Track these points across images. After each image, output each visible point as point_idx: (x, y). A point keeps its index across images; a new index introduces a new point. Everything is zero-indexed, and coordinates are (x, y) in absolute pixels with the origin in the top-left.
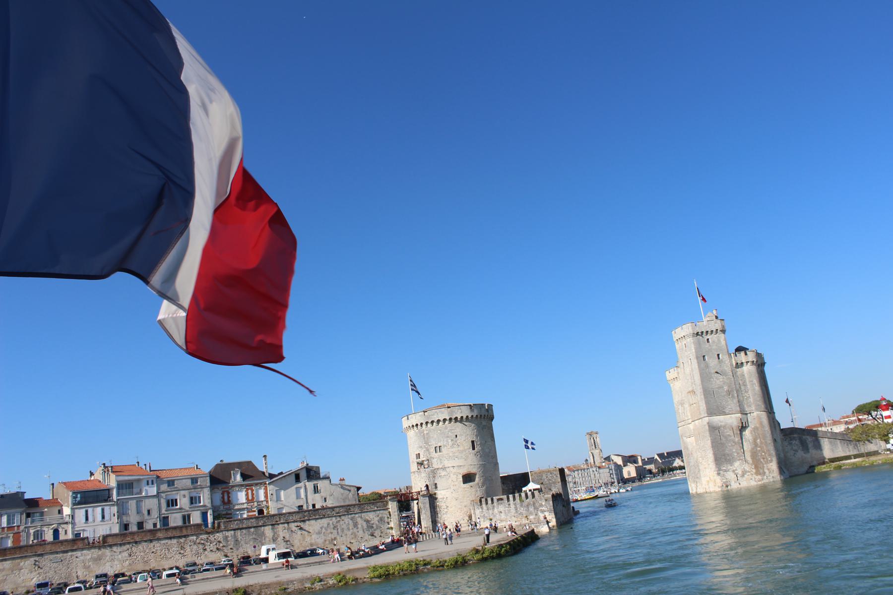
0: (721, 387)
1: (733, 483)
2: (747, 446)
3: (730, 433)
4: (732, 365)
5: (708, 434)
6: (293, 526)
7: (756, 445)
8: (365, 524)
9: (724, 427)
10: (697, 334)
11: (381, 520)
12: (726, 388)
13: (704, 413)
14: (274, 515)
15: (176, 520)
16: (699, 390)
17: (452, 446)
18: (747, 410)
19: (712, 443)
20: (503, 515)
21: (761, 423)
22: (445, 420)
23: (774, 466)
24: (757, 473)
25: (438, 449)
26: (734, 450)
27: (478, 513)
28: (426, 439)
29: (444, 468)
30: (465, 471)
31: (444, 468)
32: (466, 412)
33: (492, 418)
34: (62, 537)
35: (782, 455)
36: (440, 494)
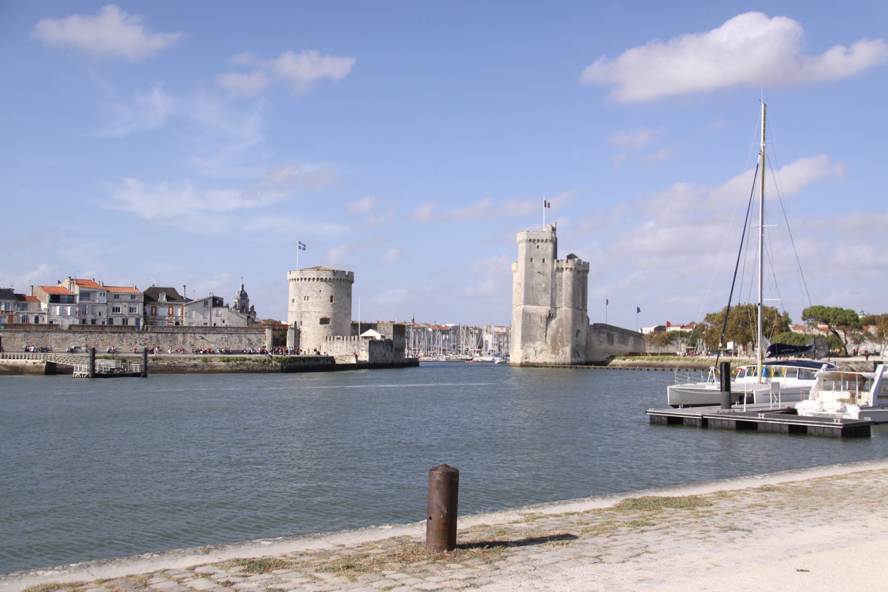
0: (540, 284)
1: (531, 357)
2: (550, 332)
3: (537, 319)
4: (553, 269)
5: (521, 317)
6: (197, 336)
7: (558, 332)
8: (247, 342)
9: (535, 314)
10: (530, 240)
11: (259, 340)
12: (543, 285)
13: (522, 303)
14: (185, 327)
15: (118, 321)
16: (523, 284)
17: (316, 298)
18: (558, 305)
19: (523, 325)
20: (338, 350)
21: (566, 317)
22: (314, 279)
23: (568, 350)
24: (552, 353)
25: (306, 298)
26: (538, 332)
27: (324, 345)
28: (299, 289)
29: (308, 312)
30: (322, 316)
31: (308, 312)
32: (329, 275)
33: (352, 282)
34: (40, 322)
35: (583, 343)
36: (303, 329)
